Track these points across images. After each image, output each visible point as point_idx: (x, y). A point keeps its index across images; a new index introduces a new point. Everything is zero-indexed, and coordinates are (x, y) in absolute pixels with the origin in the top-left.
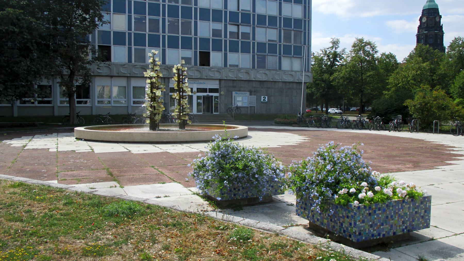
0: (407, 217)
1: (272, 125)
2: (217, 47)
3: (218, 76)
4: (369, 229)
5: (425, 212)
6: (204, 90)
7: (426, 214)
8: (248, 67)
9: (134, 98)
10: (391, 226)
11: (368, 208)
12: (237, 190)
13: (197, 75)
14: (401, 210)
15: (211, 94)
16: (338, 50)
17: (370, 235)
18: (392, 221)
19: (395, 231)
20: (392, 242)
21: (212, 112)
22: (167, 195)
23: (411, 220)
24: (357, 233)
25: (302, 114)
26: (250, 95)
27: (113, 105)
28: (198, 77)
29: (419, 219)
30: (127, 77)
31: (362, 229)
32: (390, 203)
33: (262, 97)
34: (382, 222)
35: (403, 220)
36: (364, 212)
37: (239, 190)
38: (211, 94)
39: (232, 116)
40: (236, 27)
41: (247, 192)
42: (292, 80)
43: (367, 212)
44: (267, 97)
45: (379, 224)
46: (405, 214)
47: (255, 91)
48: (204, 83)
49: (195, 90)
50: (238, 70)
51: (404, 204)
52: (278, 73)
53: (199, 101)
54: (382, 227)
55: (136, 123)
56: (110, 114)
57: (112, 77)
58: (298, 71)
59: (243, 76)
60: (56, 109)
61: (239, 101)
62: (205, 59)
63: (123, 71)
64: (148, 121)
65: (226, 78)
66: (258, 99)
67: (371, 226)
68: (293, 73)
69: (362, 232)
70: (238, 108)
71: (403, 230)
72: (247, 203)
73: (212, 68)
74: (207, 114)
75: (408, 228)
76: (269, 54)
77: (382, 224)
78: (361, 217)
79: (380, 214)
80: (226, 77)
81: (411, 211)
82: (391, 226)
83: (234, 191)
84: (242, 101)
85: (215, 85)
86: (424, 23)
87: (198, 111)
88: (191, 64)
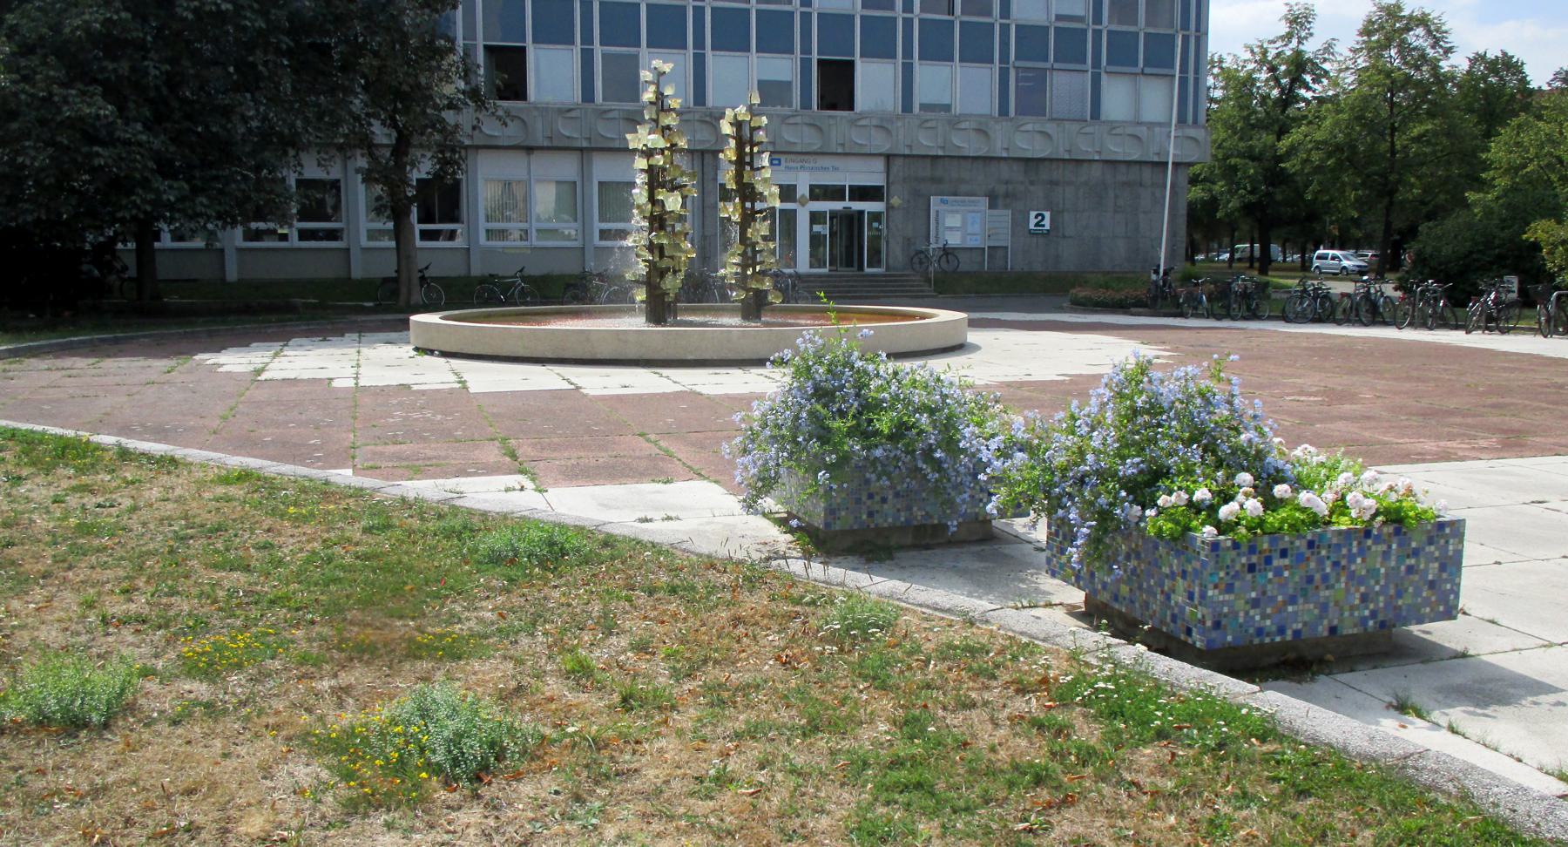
0: (1377, 583)
1: (1060, 309)
2: (880, 43)
3: (881, 143)
4: (1247, 613)
5: (1443, 568)
6: (835, 193)
7: (1445, 575)
8: (986, 111)
9: (602, 220)
10: (1324, 608)
11: (1244, 549)
12: (877, 498)
13: (812, 140)
14: (1359, 560)
15: (857, 206)
16: (1310, 48)
17: (1251, 630)
18: (1327, 593)
19: (1335, 622)
20: (1329, 657)
21: (861, 268)
22: (673, 515)
23: (1392, 592)
24: (1209, 623)
25: (1165, 273)
26: (992, 206)
27: (536, 243)
28: (815, 148)
29: (1417, 593)
30: (581, 150)
31: (1226, 610)
32: (1321, 536)
33: (1033, 214)
34: (1291, 591)
35: (1362, 589)
36: (1233, 561)
37: (884, 500)
38: (857, 206)
39: (928, 281)
41: (909, 508)
42: (1135, 156)
43: (1244, 560)
44: (1047, 215)
45: (1280, 598)
46: (1372, 572)
47: (1007, 195)
48: (836, 169)
49: (803, 190)
51: (1369, 542)
52: (1089, 130)
53: (817, 228)
54: (1290, 609)
55: (609, 301)
56: (527, 272)
57: (530, 149)
58: (1160, 124)
59: (968, 144)
60: (356, 256)
61: (951, 229)
62: (836, 86)
63: (565, 130)
64: (640, 295)
65: (907, 152)
66: (1019, 222)
67: (1255, 603)
68: (1142, 131)
69: (1224, 621)
70: (947, 251)
71: (1364, 620)
72: (909, 540)
73: (862, 116)
74: (843, 271)
75: (1381, 617)
76: (1056, 66)
77: (1292, 600)
78: (1222, 574)
79: (1286, 567)
80: (910, 147)
81: (1393, 564)
82: (1324, 608)
83: (869, 502)
87: (816, 260)
88: (790, 105)
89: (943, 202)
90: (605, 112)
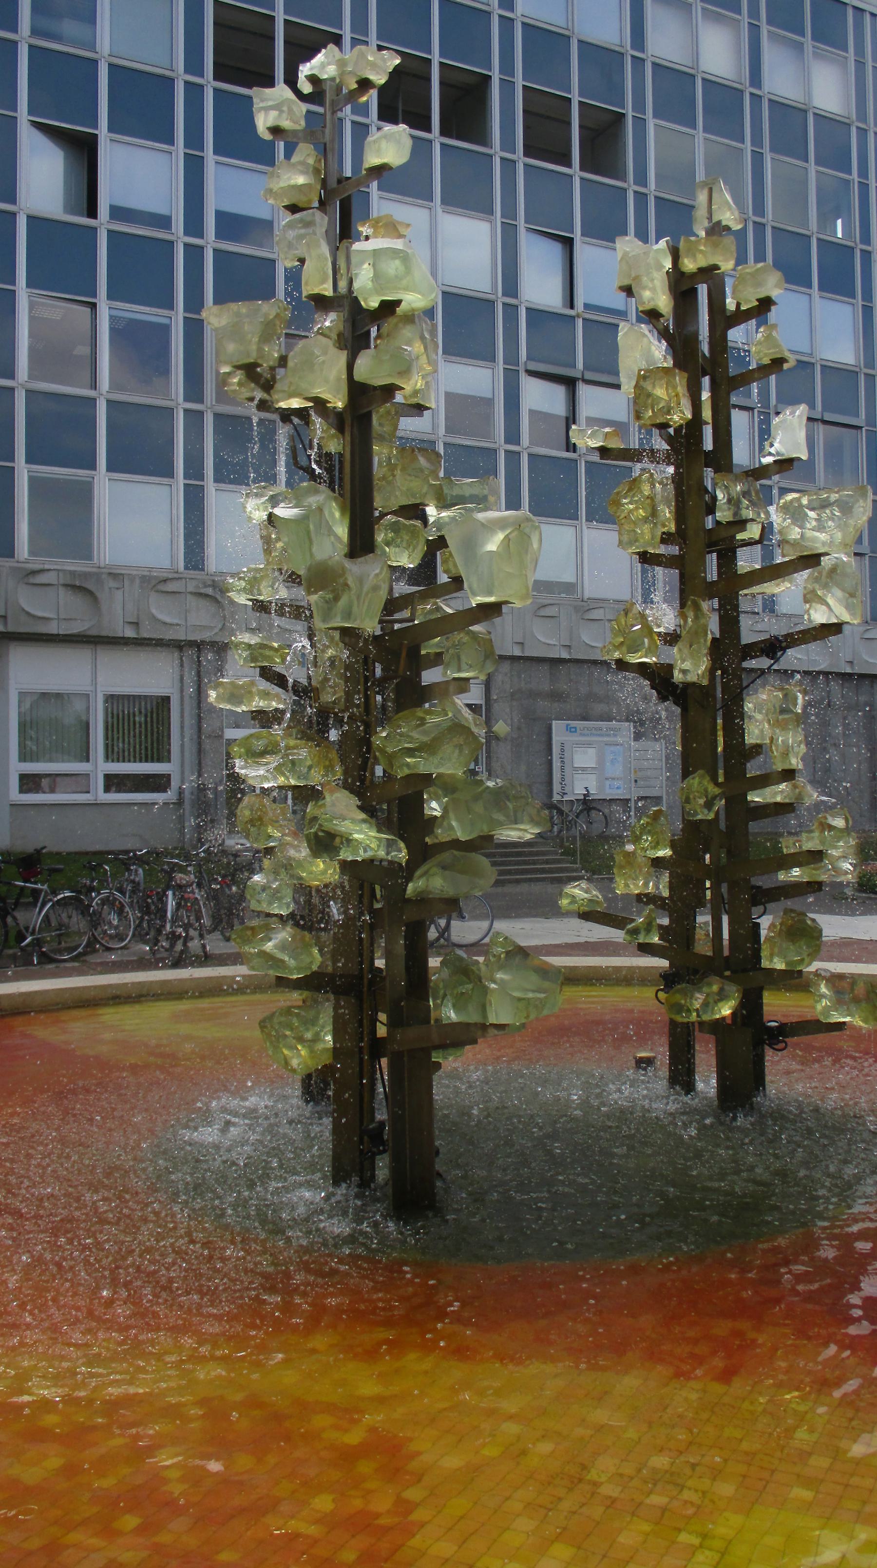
9: (24, 756)
26: (638, 737)
40: (559, 392)
50: (577, 609)
65: (517, 652)
84: (599, 769)
89: (571, 730)
90: (34, 573)
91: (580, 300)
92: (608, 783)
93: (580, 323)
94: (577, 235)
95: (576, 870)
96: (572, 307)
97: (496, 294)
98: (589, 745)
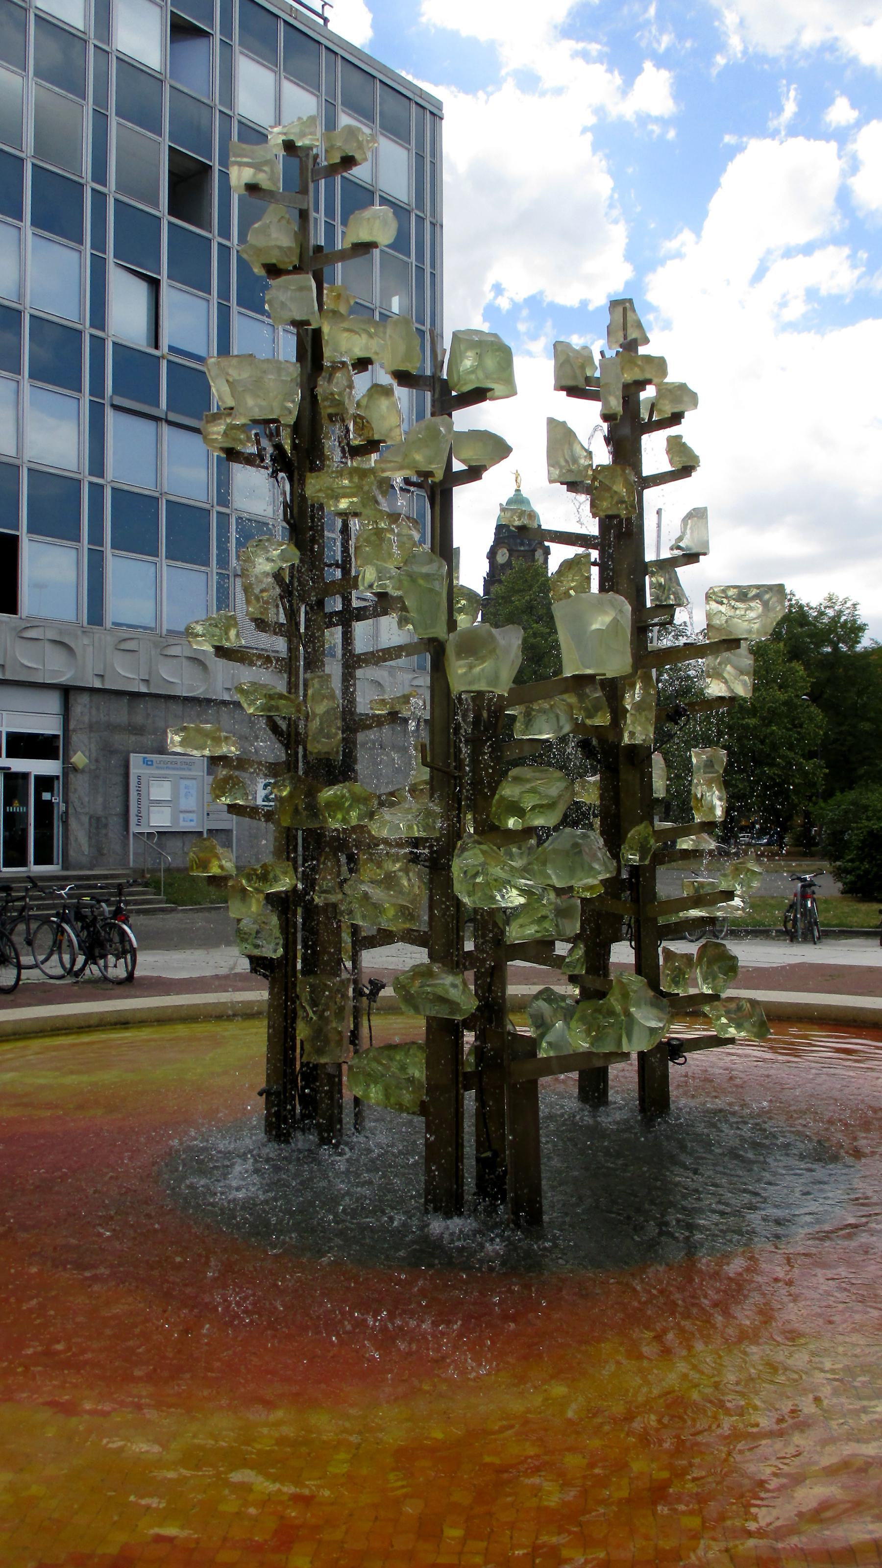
61: (159, 802)
65: (98, 684)
85: (43, 720)
86: (502, 565)
89: (146, 762)
91: (165, 341)
92: (182, 816)
93: (164, 365)
94: (164, 278)
95: (160, 902)
96: (157, 347)
97: (84, 324)
98: (164, 778)
